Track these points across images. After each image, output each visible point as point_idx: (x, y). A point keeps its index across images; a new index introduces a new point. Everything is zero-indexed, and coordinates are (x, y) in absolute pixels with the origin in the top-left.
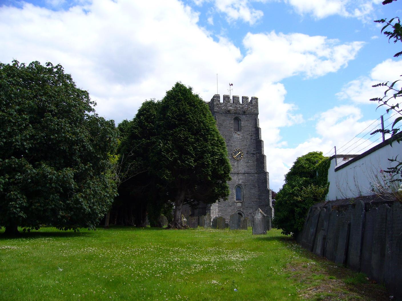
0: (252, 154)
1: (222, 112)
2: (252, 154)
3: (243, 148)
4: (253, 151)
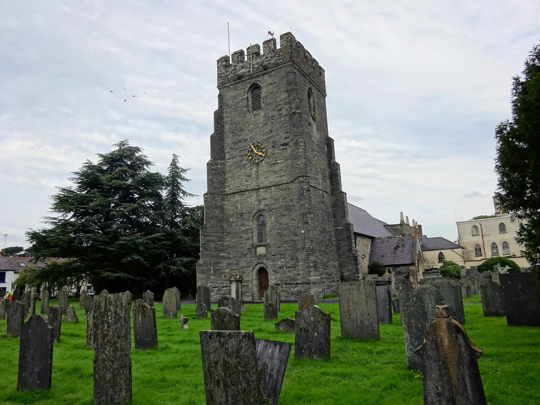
0: (282, 145)
1: (228, 84)
2: (282, 145)
3: (265, 137)
4: (285, 138)
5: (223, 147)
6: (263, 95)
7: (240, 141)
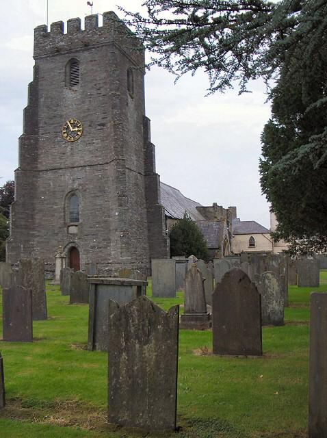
3: (82, 115)
4: (103, 118)
6: (81, 71)
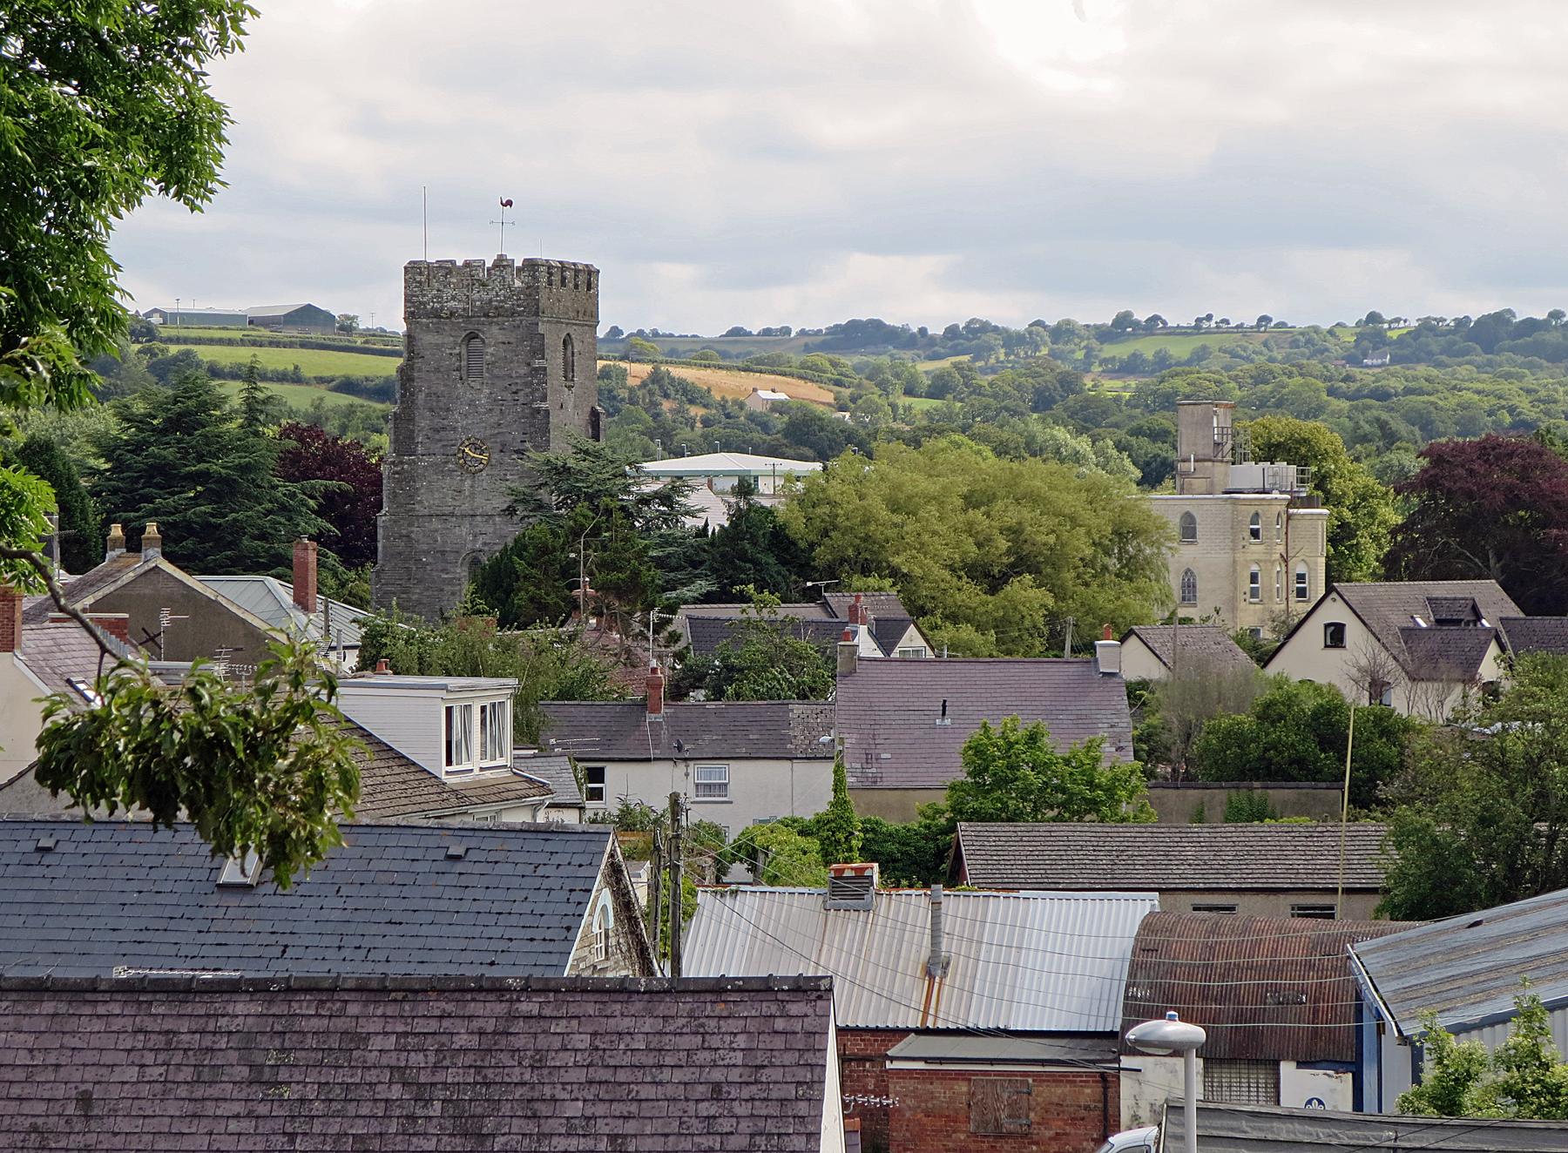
3: (488, 432)
5: (413, 431)
7: (444, 429)
